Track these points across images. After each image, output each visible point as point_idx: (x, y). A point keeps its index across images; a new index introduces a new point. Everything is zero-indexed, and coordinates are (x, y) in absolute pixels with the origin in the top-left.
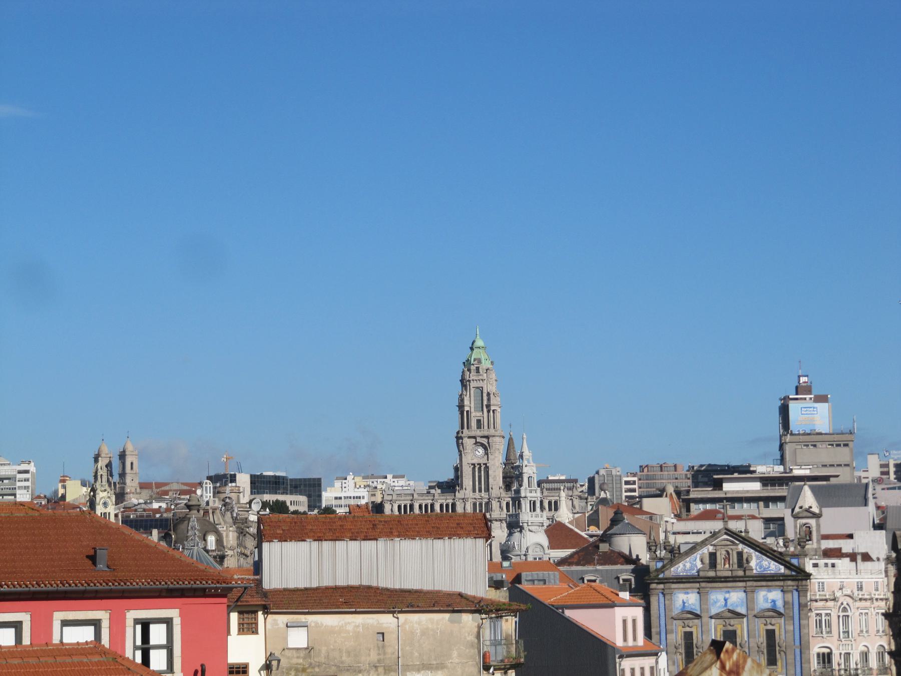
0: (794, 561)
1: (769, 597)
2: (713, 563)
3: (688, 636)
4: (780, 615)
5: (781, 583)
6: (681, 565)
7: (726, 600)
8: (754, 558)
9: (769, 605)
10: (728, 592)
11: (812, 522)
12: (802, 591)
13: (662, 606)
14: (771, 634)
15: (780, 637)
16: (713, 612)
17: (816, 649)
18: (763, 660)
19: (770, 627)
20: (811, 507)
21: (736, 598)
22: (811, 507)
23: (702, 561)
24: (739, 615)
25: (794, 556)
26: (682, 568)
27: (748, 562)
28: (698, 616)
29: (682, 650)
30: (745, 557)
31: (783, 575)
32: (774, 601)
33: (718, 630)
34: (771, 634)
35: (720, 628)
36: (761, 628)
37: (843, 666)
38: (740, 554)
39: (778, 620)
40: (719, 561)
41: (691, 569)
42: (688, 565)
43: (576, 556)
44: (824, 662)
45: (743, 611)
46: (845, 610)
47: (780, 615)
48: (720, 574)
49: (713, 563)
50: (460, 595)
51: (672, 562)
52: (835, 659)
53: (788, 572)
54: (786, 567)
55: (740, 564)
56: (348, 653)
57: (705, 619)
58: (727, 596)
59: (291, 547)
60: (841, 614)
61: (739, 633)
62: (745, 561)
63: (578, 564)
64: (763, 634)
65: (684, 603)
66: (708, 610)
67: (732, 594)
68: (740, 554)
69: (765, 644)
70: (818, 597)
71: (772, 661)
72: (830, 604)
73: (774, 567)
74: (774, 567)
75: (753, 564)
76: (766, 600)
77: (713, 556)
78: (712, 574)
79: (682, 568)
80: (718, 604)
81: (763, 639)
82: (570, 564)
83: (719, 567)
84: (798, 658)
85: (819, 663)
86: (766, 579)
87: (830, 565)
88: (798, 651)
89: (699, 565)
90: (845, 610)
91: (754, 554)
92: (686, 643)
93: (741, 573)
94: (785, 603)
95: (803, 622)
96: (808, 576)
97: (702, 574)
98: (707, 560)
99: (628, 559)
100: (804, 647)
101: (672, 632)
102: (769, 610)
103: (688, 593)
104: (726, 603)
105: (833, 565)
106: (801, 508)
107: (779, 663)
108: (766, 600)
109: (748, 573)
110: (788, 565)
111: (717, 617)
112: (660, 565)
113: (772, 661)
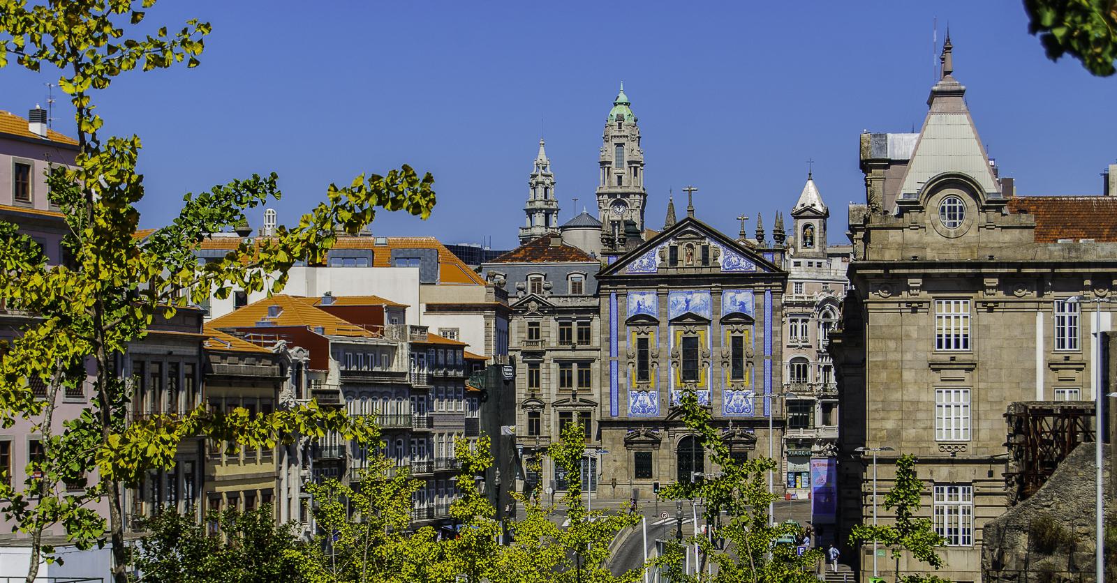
0: (768, 257)
3: (643, 343)
4: (749, 320)
7: (687, 302)
8: (722, 253)
9: (736, 309)
10: (691, 293)
11: (816, 223)
13: (614, 308)
14: (737, 343)
15: (749, 346)
18: (728, 372)
19: (737, 334)
20: (814, 205)
21: (699, 299)
22: (814, 205)
26: (640, 265)
27: (715, 259)
29: (636, 360)
31: (754, 275)
32: (742, 304)
33: (678, 336)
34: (737, 343)
35: (680, 335)
36: (727, 334)
38: (705, 249)
39: (747, 327)
41: (649, 265)
42: (645, 261)
43: (523, 252)
44: (799, 375)
45: (706, 314)
47: (749, 320)
48: (680, 272)
49: (674, 261)
51: (628, 258)
54: (757, 264)
55: (705, 260)
57: (664, 324)
58: (689, 297)
62: (711, 256)
63: (522, 260)
64: (730, 341)
65: (639, 305)
66: (667, 314)
67: (695, 295)
68: (705, 249)
70: (794, 300)
71: (738, 374)
73: (743, 265)
74: (743, 265)
75: (720, 260)
77: (674, 250)
78: (672, 272)
79: (640, 265)
80: (679, 307)
81: (728, 349)
82: (515, 259)
84: (768, 369)
85: (792, 376)
87: (815, 265)
88: (768, 362)
89: (658, 260)
92: (639, 352)
93: (706, 271)
94: (757, 306)
99: (580, 255)
100: (776, 357)
101: (624, 338)
103: (644, 294)
104: (688, 306)
105: (819, 265)
106: (803, 205)
107: (746, 376)
109: (715, 271)
110: (761, 263)
111: (678, 321)
112: (613, 260)
113: (738, 374)
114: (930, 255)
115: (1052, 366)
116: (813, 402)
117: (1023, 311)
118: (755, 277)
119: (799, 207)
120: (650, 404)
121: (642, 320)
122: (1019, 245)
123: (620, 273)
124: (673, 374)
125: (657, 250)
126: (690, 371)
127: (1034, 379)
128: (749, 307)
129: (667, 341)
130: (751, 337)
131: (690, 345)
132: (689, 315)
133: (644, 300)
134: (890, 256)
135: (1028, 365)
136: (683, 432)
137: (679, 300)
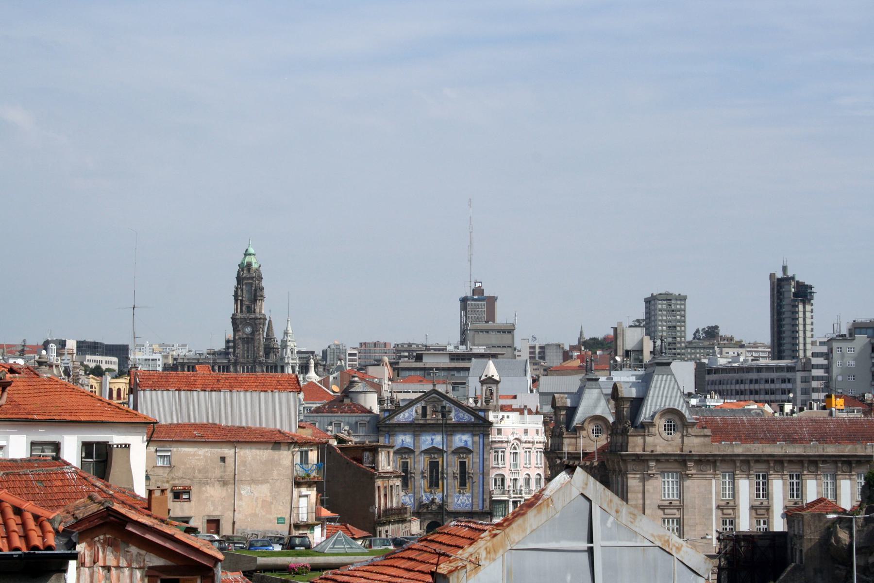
0: (481, 414)
1: (461, 439)
2: (424, 414)
5: (471, 429)
6: (402, 414)
7: (432, 440)
9: (462, 445)
12: (486, 435)
14: (463, 465)
16: (424, 447)
17: (493, 474)
18: (457, 483)
21: (438, 440)
23: (416, 412)
24: (441, 452)
25: (481, 410)
26: (404, 417)
28: (412, 452)
30: (447, 409)
32: (466, 441)
34: (463, 465)
37: (511, 489)
40: (428, 413)
41: (409, 417)
42: (407, 415)
46: (515, 448)
48: (429, 422)
49: (424, 414)
50: (280, 431)
52: (508, 483)
53: (477, 422)
56: (200, 471)
59: (158, 395)
60: (513, 451)
61: (440, 463)
68: (444, 407)
69: (458, 472)
71: (463, 484)
72: (505, 445)
74: (466, 418)
76: (461, 440)
77: (424, 409)
79: (404, 417)
81: (457, 470)
83: (428, 417)
86: (461, 427)
90: (515, 448)
91: (454, 409)
94: (473, 443)
95: (485, 456)
96: (491, 424)
97: (416, 422)
98: (420, 411)
100: (484, 474)
102: (461, 448)
108: (461, 440)
109: (449, 422)
111: (426, 452)
112: (387, 414)
113: (463, 484)
114: (659, 450)
115: (718, 507)
116: (508, 501)
117: (706, 479)
118: (474, 425)
119: (483, 378)
120: (409, 502)
121: (404, 451)
122: (704, 445)
123: (392, 422)
124: (423, 483)
125: (414, 408)
126: (434, 483)
127: (712, 515)
128: (470, 443)
129: (421, 464)
130: (472, 462)
131: (434, 466)
132: (434, 448)
133: (404, 439)
134: (639, 450)
135: (708, 506)
136: (430, 519)
137: (428, 440)
